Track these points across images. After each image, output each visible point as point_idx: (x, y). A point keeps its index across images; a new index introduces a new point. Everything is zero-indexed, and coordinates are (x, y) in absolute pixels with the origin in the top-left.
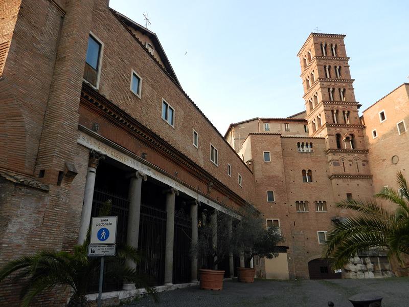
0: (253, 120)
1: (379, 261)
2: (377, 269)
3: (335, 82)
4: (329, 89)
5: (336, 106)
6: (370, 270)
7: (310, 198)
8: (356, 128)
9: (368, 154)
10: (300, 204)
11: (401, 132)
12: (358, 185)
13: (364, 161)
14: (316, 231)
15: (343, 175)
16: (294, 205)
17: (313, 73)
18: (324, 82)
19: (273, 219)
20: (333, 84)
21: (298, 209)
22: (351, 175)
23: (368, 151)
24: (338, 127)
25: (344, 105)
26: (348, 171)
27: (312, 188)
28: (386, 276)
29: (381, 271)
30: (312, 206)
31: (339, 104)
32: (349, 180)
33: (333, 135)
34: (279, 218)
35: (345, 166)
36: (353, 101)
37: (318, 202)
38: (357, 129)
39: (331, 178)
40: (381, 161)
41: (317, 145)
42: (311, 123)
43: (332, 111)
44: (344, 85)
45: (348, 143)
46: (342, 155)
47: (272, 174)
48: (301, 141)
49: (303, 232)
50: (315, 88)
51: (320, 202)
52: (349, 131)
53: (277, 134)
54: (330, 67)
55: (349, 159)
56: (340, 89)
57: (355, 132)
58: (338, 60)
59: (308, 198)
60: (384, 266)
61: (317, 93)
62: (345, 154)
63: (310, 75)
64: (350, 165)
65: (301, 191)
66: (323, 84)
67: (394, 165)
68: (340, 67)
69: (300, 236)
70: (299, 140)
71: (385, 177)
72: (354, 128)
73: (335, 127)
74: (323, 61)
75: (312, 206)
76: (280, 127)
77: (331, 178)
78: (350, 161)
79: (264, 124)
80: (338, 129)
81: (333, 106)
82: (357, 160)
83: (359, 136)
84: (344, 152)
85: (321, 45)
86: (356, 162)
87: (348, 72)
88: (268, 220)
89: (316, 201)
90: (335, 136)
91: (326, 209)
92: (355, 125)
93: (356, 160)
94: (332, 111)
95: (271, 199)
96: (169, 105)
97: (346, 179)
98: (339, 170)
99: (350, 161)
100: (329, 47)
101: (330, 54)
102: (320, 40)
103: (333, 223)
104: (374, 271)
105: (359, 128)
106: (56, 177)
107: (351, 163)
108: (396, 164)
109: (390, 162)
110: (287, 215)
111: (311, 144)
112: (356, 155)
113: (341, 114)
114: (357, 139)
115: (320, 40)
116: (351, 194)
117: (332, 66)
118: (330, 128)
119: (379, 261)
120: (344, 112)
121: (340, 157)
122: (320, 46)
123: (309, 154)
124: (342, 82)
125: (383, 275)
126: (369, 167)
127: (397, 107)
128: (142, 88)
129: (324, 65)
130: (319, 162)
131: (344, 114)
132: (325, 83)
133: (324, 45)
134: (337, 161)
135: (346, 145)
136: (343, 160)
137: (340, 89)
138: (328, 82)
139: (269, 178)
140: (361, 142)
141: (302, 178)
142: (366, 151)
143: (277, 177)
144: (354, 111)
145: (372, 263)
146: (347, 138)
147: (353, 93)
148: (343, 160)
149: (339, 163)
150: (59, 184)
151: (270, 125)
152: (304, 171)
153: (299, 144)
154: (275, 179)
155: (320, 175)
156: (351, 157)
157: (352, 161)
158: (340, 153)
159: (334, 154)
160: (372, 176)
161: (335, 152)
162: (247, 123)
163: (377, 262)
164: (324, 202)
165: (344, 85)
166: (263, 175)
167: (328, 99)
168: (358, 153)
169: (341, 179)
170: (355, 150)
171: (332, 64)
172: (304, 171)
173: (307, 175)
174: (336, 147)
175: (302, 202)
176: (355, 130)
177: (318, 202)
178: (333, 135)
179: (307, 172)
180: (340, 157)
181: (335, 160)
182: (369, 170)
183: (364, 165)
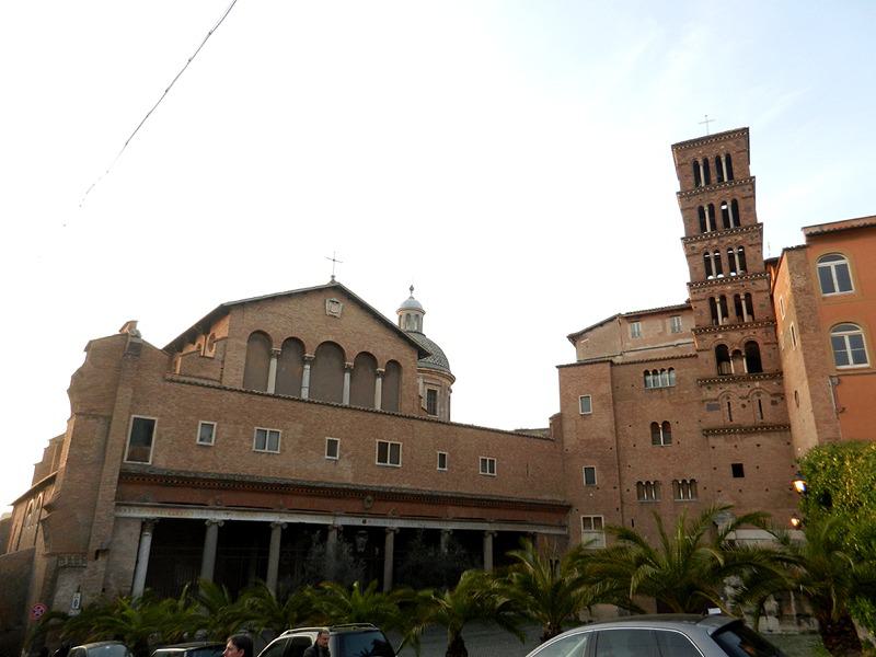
0: (611, 320)
1: (793, 597)
2: (786, 612)
5: (719, 288)
6: (770, 613)
7: (664, 475)
10: (644, 487)
16: (634, 489)
19: (592, 516)
20: (715, 242)
21: (640, 496)
22: (740, 428)
23: (781, 373)
24: (720, 331)
26: (737, 420)
27: (668, 456)
28: (806, 626)
29: (798, 615)
32: (738, 436)
39: (709, 432)
44: (740, 238)
47: (594, 435)
48: (650, 367)
51: (684, 481)
57: (758, 335)
60: (803, 609)
62: (732, 385)
64: (744, 406)
65: (645, 463)
66: (693, 248)
74: (695, 198)
76: (661, 327)
77: (709, 432)
79: (629, 326)
80: (720, 336)
81: (712, 288)
82: (758, 394)
83: (765, 344)
84: (729, 382)
86: (756, 398)
87: (751, 209)
89: (677, 481)
91: (695, 494)
93: (758, 394)
95: (591, 480)
96: (268, 430)
98: (717, 419)
100: (712, 165)
101: (714, 178)
102: (692, 154)
104: (780, 615)
105: (768, 325)
106: (94, 554)
107: (745, 402)
112: (757, 384)
114: (764, 351)
115: (692, 154)
116: (741, 465)
118: (703, 336)
119: (793, 597)
124: (735, 234)
125: (799, 624)
126: (786, 405)
128: (217, 433)
130: (685, 404)
132: (697, 245)
134: (716, 400)
139: (588, 443)
143: (601, 440)
145: (776, 600)
150: (96, 558)
151: (639, 326)
152: (654, 425)
153: (647, 373)
154: (598, 444)
155: (686, 430)
156: (745, 390)
157: (747, 397)
159: (709, 388)
162: (601, 328)
163: (789, 600)
164: (692, 481)
165: (740, 238)
172: (654, 425)
173: (662, 430)
174: (713, 372)
175: (648, 483)
180: (720, 391)
181: (711, 400)
182: (786, 413)
183: (774, 403)
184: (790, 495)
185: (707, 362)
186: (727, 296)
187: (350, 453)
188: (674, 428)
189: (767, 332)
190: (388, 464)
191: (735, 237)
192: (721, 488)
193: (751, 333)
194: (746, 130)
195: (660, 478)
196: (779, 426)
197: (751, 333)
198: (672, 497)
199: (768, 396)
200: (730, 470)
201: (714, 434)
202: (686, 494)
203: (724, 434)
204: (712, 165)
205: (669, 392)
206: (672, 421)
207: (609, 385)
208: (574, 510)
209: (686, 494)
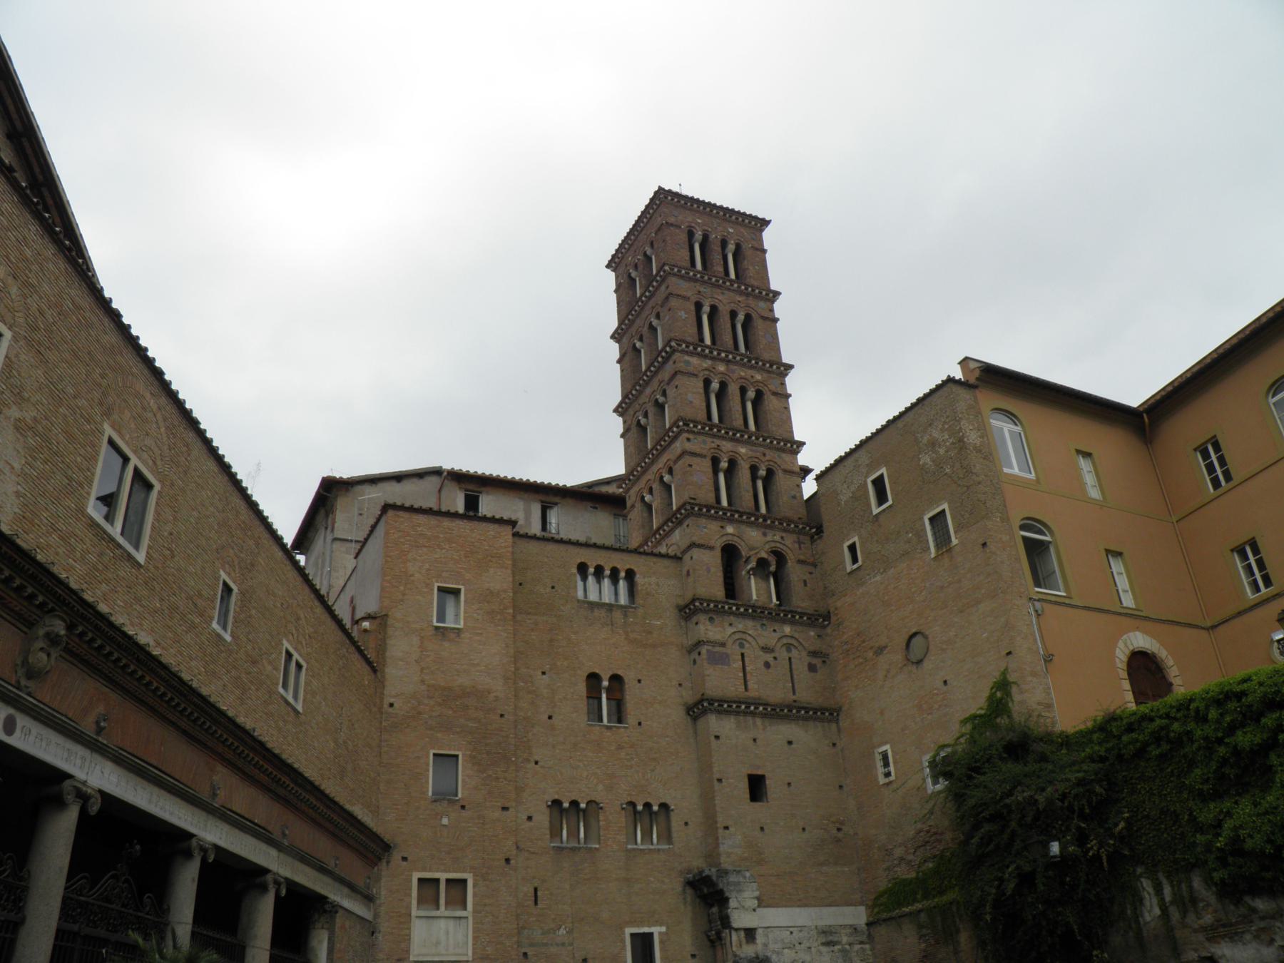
3: (728, 362)
4: (707, 383)
5: (727, 446)
8: (793, 532)
9: (829, 630)
11: (938, 547)
12: (790, 743)
13: (814, 654)
14: (621, 928)
15: (739, 703)
16: (543, 818)
17: (655, 322)
18: (691, 354)
19: (443, 876)
21: (555, 832)
22: (766, 705)
23: (827, 617)
24: (731, 520)
25: (754, 444)
26: (755, 690)
27: (620, 748)
30: (613, 820)
31: (737, 441)
32: (759, 721)
33: (712, 548)
34: (473, 869)
35: (748, 669)
36: (786, 436)
37: (640, 808)
38: (794, 537)
40: (870, 654)
41: (653, 580)
42: (639, 505)
43: (715, 461)
44: (758, 377)
45: (763, 584)
46: (741, 625)
48: (593, 559)
49: (570, 932)
50: (660, 377)
51: (648, 806)
52: (769, 538)
53: (501, 521)
54: (714, 309)
55: (762, 642)
56: (743, 391)
58: (741, 293)
59: (600, 787)
61: (664, 394)
62: (750, 623)
63: (645, 330)
67: (914, 668)
68: (748, 318)
69: (553, 950)
70: (593, 559)
71: (882, 713)
72: (785, 530)
73: (721, 519)
75: (613, 820)
78: (766, 649)
80: (730, 529)
81: (718, 442)
82: (789, 650)
83: (801, 562)
84: (744, 615)
85: (691, 234)
88: (420, 880)
90: (718, 553)
91: (667, 836)
92: (790, 521)
94: (715, 461)
97: (750, 719)
98: (721, 682)
99: (766, 649)
100: (716, 247)
103: (689, 891)
105: (801, 532)
107: (769, 658)
108: (919, 662)
109: (898, 657)
110: (507, 861)
111: (630, 575)
112: (787, 629)
113: (744, 475)
114: (795, 573)
117: (724, 310)
120: (754, 469)
121: (730, 630)
122: (683, 237)
123: (617, 615)
124: (752, 367)
127: (926, 459)
129: (694, 299)
131: (754, 478)
133: (699, 235)
134: (723, 645)
135: (757, 590)
136: (742, 646)
137: (743, 391)
138: (706, 357)
140: (805, 582)
141: (583, 705)
142: (820, 619)
144: (785, 471)
146: (762, 563)
147: (787, 409)
148: (742, 646)
149: (727, 655)
152: (593, 678)
158: (732, 618)
159: (711, 619)
160: (839, 710)
161: (722, 612)
164: (664, 806)
165: (758, 377)
166: (423, 681)
167: (702, 416)
168: (792, 622)
169: (732, 719)
170: (782, 613)
171: (725, 301)
172: (593, 678)
174: (719, 592)
175: (574, 804)
176: (790, 540)
177: (640, 808)
178: (712, 548)
179: (605, 683)
180: (730, 630)
183: (812, 668)
184: (838, 841)
185: (708, 570)
186: (740, 461)
187: (29, 414)
188: (632, 695)
189: (800, 543)
190: (115, 530)
191: (750, 372)
192: (729, 823)
193: (777, 538)
194: (768, 222)
195: (599, 795)
196: (823, 710)
197: (777, 538)
198: (622, 838)
199: (804, 653)
200: (744, 786)
201: (720, 712)
202: (647, 835)
203: (737, 713)
204: (716, 247)
205: (625, 615)
206: (629, 677)
207: (509, 571)
208: (396, 856)
209: (647, 835)
